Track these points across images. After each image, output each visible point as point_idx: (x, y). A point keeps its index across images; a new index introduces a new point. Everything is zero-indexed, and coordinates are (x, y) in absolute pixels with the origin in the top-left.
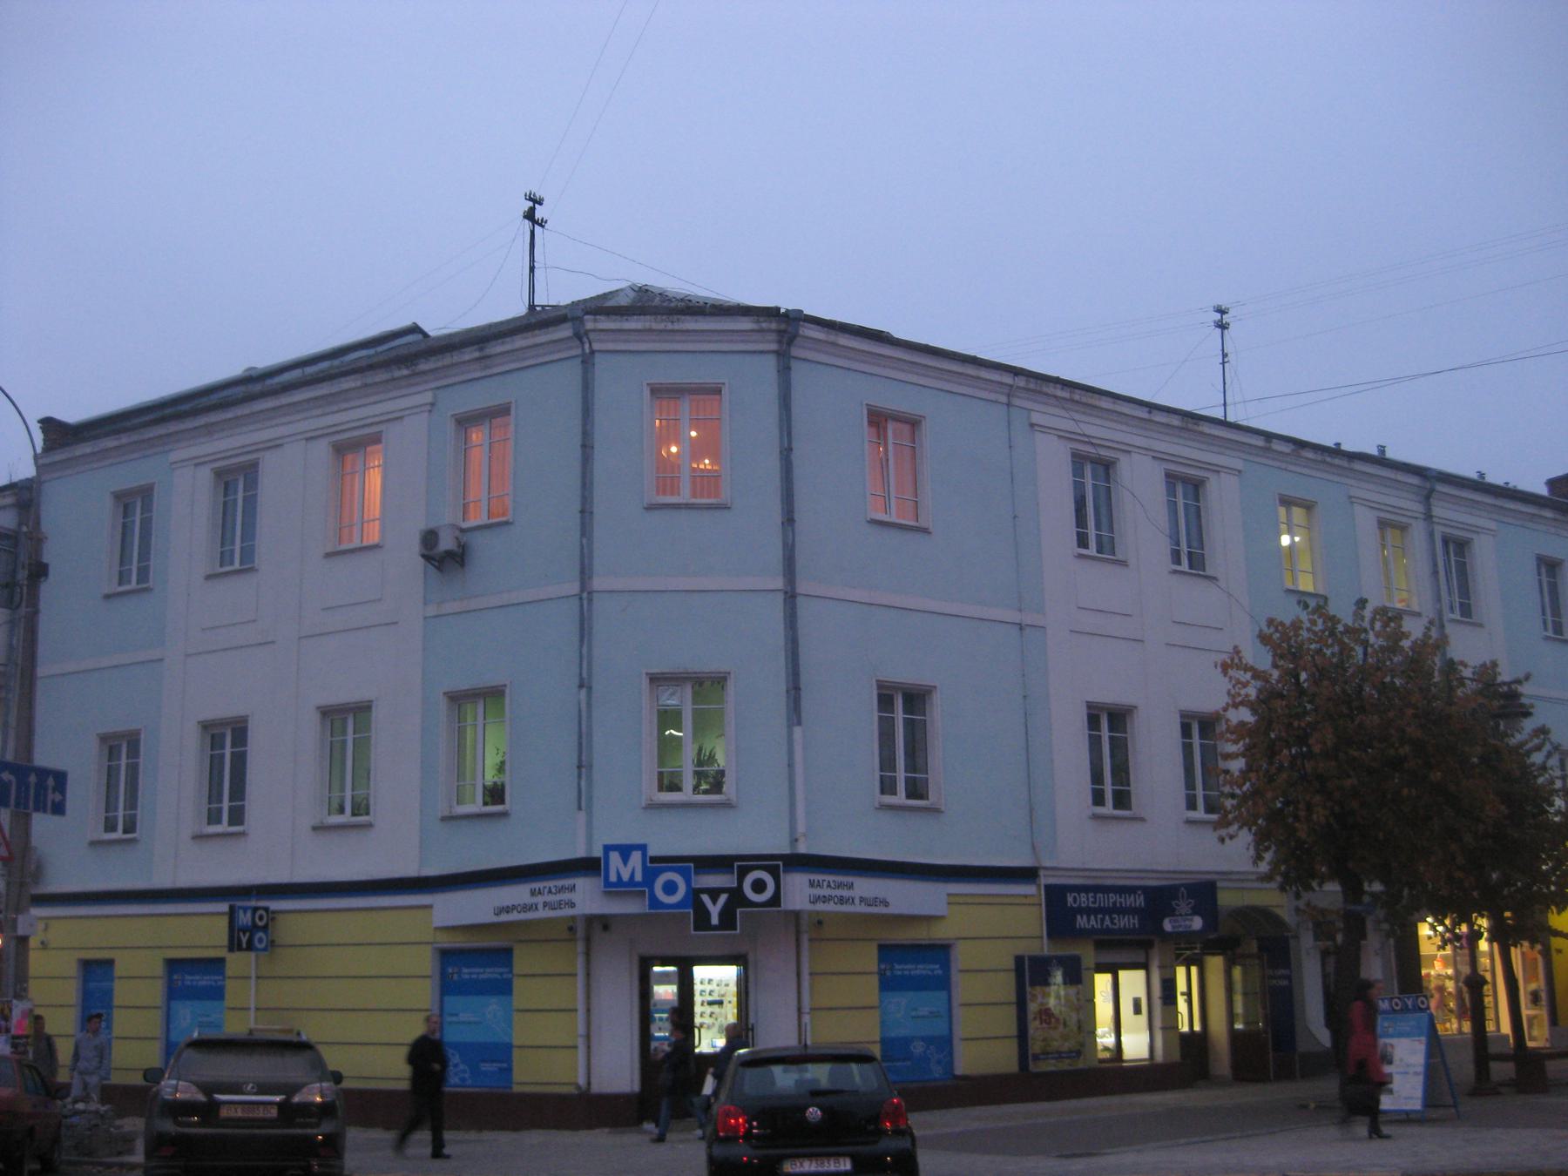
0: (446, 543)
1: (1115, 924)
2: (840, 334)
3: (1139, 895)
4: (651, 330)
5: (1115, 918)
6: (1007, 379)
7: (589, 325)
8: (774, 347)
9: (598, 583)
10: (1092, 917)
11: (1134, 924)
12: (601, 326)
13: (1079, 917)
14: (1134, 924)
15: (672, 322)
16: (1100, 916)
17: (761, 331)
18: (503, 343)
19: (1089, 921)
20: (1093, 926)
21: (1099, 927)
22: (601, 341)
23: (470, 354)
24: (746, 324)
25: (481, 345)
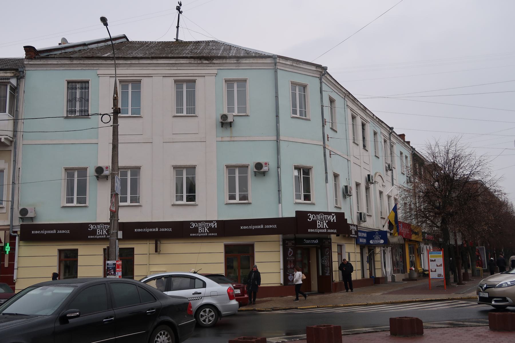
0: (230, 120)
4: (292, 65)
7: (278, 61)
9: (281, 138)
12: (281, 61)
15: (297, 64)
18: (246, 60)
22: (279, 66)
23: (234, 61)
25: (237, 59)
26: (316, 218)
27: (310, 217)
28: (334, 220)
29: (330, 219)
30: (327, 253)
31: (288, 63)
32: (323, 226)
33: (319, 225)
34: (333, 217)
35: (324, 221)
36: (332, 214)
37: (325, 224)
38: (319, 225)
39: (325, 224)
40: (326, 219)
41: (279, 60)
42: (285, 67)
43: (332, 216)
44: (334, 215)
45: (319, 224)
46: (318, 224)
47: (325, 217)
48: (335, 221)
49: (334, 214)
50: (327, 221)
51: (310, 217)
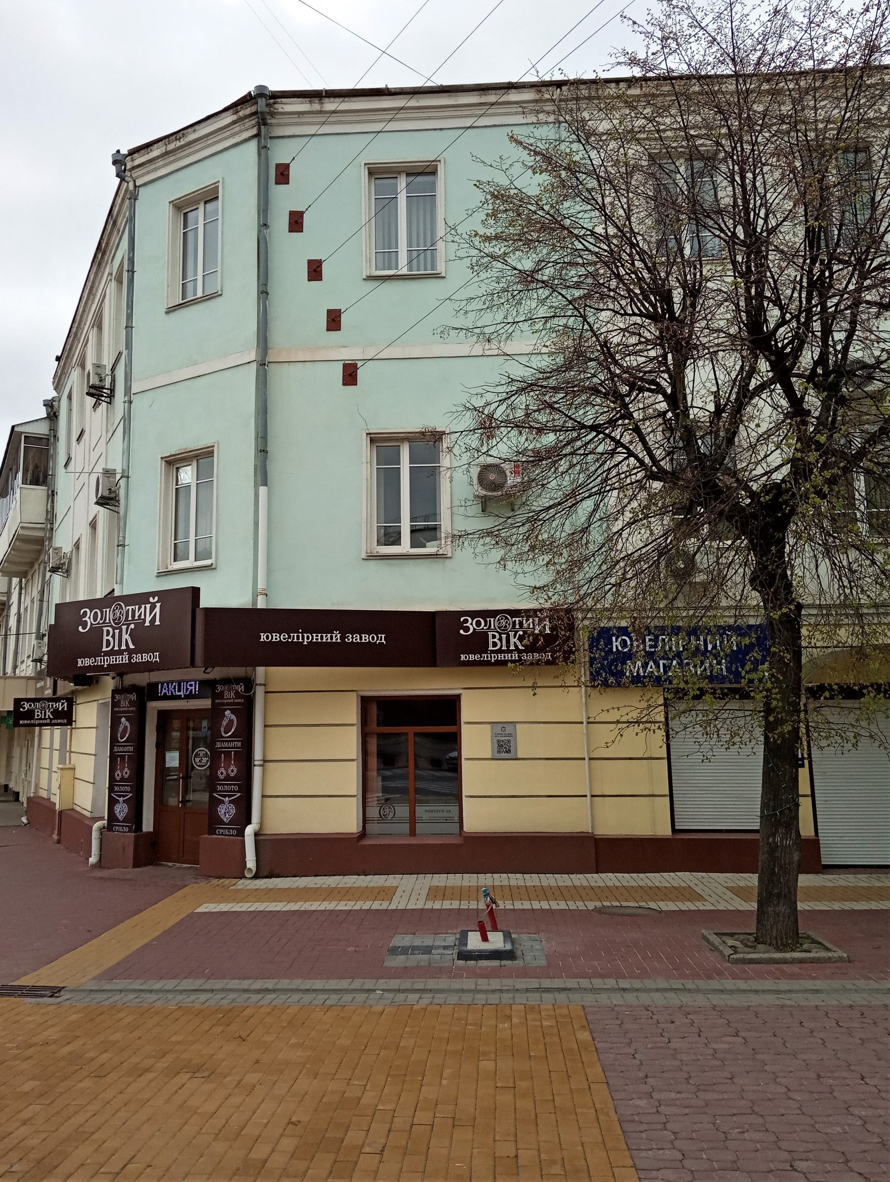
2: (327, 100)
8: (254, 131)
12: (137, 162)
17: (241, 119)
22: (138, 177)
24: (229, 118)
26: (101, 619)
27: (86, 619)
28: (153, 620)
29: (143, 617)
30: (226, 733)
31: (156, 152)
32: (120, 645)
33: (108, 641)
34: (153, 607)
35: (124, 627)
36: (151, 600)
37: (125, 636)
38: (108, 641)
39: (125, 636)
40: (130, 618)
41: (133, 160)
42: (156, 170)
43: (148, 606)
44: (157, 602)
45: (109, 638)
46: (105, 638)
47: (128, 612)
48: (157, 623)
49: (156, 598)
50: (132, 626)
51: (86, 619)
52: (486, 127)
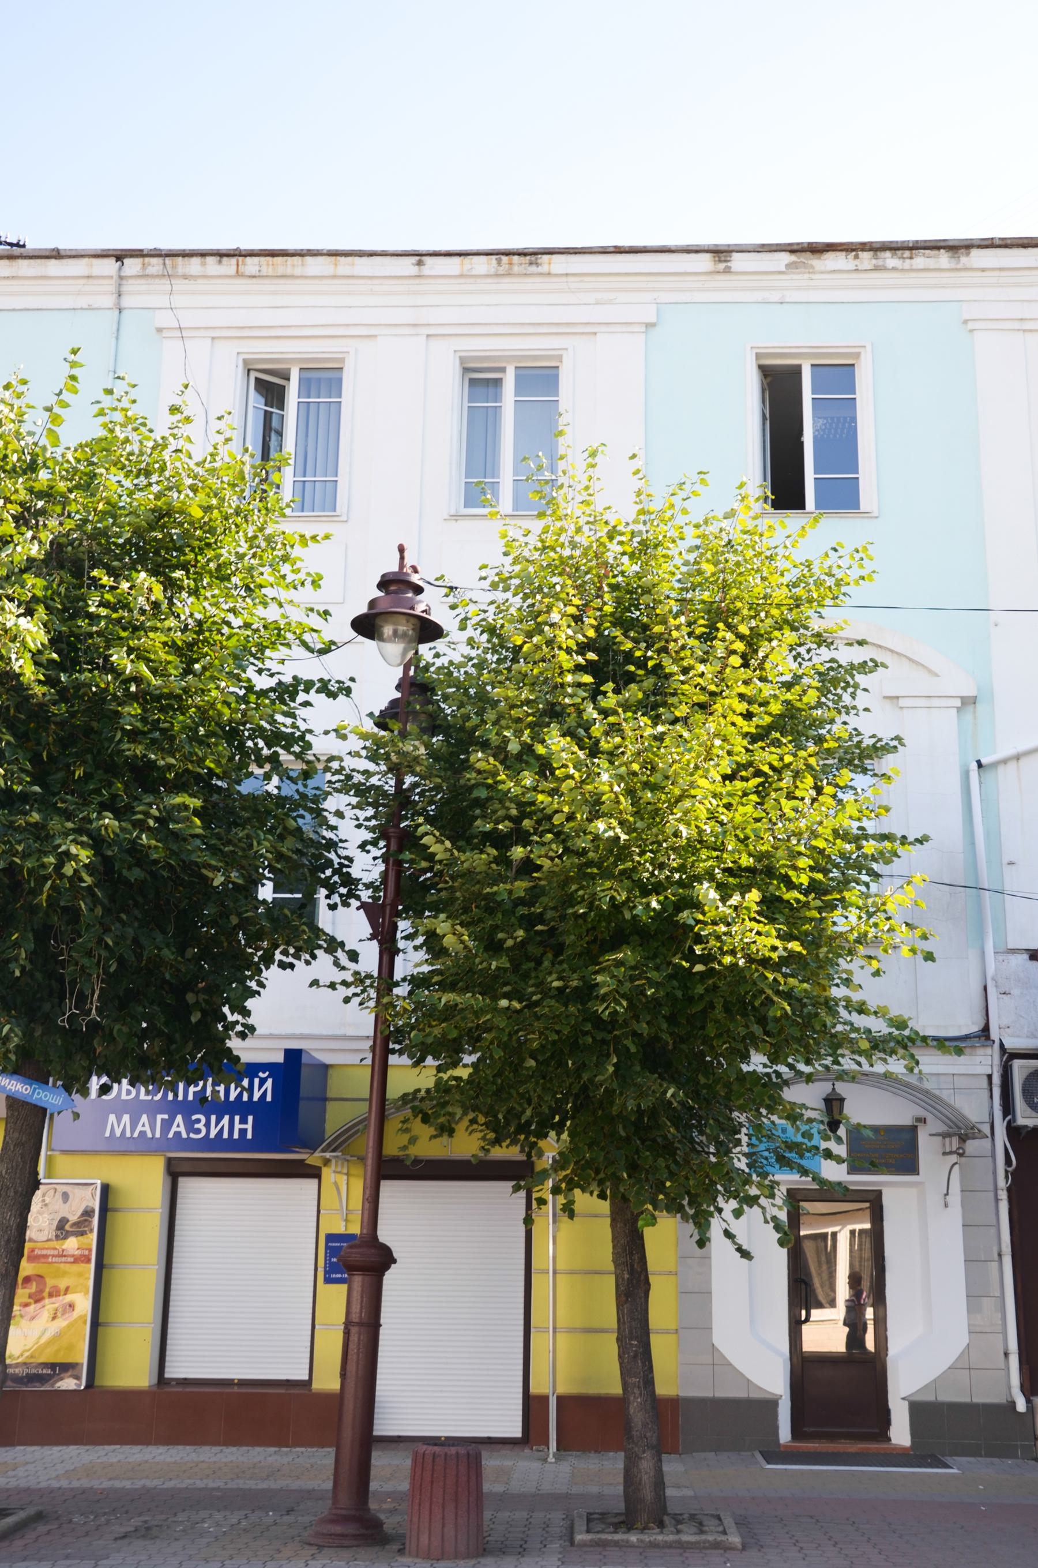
1: (199, 1131)
3: (263, 1082)
5: (198, 1121)
6: (110, 266)
10: (144, 1118)
11: (243, 1132)
13: (112, 1118)
14: (243, 1132)
16: (159, 1117)
19: (134, 1124)
20: (142, 1133)
21: (158, 1135)
52: (14, 310)
